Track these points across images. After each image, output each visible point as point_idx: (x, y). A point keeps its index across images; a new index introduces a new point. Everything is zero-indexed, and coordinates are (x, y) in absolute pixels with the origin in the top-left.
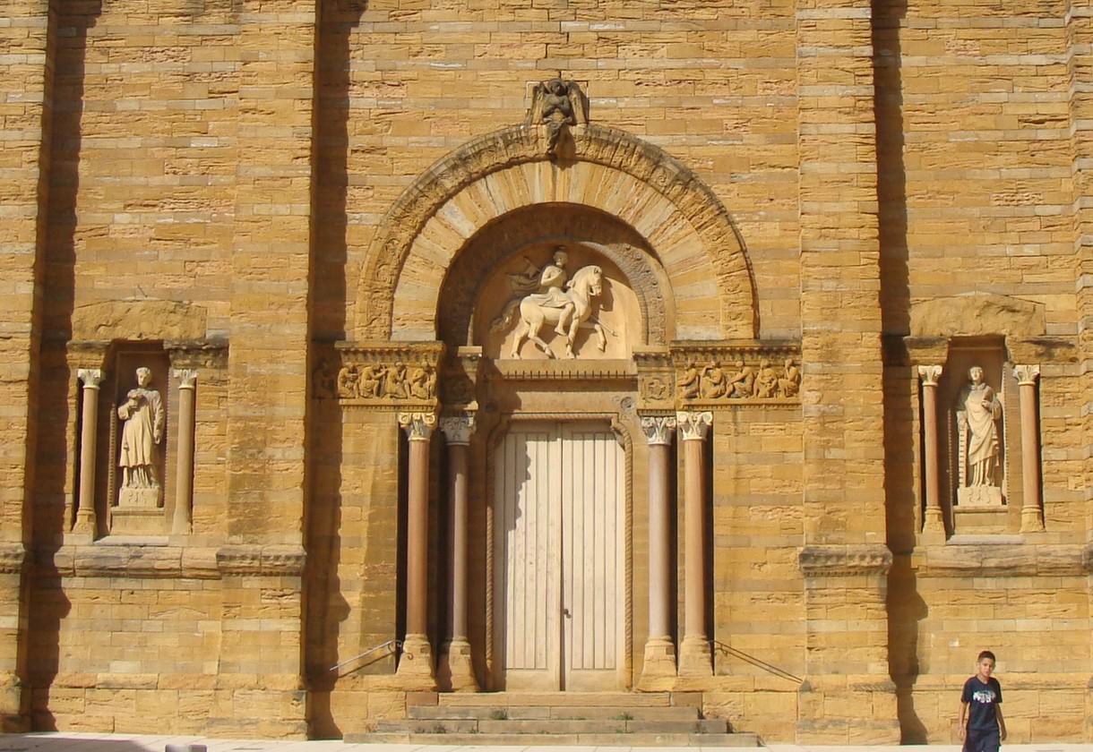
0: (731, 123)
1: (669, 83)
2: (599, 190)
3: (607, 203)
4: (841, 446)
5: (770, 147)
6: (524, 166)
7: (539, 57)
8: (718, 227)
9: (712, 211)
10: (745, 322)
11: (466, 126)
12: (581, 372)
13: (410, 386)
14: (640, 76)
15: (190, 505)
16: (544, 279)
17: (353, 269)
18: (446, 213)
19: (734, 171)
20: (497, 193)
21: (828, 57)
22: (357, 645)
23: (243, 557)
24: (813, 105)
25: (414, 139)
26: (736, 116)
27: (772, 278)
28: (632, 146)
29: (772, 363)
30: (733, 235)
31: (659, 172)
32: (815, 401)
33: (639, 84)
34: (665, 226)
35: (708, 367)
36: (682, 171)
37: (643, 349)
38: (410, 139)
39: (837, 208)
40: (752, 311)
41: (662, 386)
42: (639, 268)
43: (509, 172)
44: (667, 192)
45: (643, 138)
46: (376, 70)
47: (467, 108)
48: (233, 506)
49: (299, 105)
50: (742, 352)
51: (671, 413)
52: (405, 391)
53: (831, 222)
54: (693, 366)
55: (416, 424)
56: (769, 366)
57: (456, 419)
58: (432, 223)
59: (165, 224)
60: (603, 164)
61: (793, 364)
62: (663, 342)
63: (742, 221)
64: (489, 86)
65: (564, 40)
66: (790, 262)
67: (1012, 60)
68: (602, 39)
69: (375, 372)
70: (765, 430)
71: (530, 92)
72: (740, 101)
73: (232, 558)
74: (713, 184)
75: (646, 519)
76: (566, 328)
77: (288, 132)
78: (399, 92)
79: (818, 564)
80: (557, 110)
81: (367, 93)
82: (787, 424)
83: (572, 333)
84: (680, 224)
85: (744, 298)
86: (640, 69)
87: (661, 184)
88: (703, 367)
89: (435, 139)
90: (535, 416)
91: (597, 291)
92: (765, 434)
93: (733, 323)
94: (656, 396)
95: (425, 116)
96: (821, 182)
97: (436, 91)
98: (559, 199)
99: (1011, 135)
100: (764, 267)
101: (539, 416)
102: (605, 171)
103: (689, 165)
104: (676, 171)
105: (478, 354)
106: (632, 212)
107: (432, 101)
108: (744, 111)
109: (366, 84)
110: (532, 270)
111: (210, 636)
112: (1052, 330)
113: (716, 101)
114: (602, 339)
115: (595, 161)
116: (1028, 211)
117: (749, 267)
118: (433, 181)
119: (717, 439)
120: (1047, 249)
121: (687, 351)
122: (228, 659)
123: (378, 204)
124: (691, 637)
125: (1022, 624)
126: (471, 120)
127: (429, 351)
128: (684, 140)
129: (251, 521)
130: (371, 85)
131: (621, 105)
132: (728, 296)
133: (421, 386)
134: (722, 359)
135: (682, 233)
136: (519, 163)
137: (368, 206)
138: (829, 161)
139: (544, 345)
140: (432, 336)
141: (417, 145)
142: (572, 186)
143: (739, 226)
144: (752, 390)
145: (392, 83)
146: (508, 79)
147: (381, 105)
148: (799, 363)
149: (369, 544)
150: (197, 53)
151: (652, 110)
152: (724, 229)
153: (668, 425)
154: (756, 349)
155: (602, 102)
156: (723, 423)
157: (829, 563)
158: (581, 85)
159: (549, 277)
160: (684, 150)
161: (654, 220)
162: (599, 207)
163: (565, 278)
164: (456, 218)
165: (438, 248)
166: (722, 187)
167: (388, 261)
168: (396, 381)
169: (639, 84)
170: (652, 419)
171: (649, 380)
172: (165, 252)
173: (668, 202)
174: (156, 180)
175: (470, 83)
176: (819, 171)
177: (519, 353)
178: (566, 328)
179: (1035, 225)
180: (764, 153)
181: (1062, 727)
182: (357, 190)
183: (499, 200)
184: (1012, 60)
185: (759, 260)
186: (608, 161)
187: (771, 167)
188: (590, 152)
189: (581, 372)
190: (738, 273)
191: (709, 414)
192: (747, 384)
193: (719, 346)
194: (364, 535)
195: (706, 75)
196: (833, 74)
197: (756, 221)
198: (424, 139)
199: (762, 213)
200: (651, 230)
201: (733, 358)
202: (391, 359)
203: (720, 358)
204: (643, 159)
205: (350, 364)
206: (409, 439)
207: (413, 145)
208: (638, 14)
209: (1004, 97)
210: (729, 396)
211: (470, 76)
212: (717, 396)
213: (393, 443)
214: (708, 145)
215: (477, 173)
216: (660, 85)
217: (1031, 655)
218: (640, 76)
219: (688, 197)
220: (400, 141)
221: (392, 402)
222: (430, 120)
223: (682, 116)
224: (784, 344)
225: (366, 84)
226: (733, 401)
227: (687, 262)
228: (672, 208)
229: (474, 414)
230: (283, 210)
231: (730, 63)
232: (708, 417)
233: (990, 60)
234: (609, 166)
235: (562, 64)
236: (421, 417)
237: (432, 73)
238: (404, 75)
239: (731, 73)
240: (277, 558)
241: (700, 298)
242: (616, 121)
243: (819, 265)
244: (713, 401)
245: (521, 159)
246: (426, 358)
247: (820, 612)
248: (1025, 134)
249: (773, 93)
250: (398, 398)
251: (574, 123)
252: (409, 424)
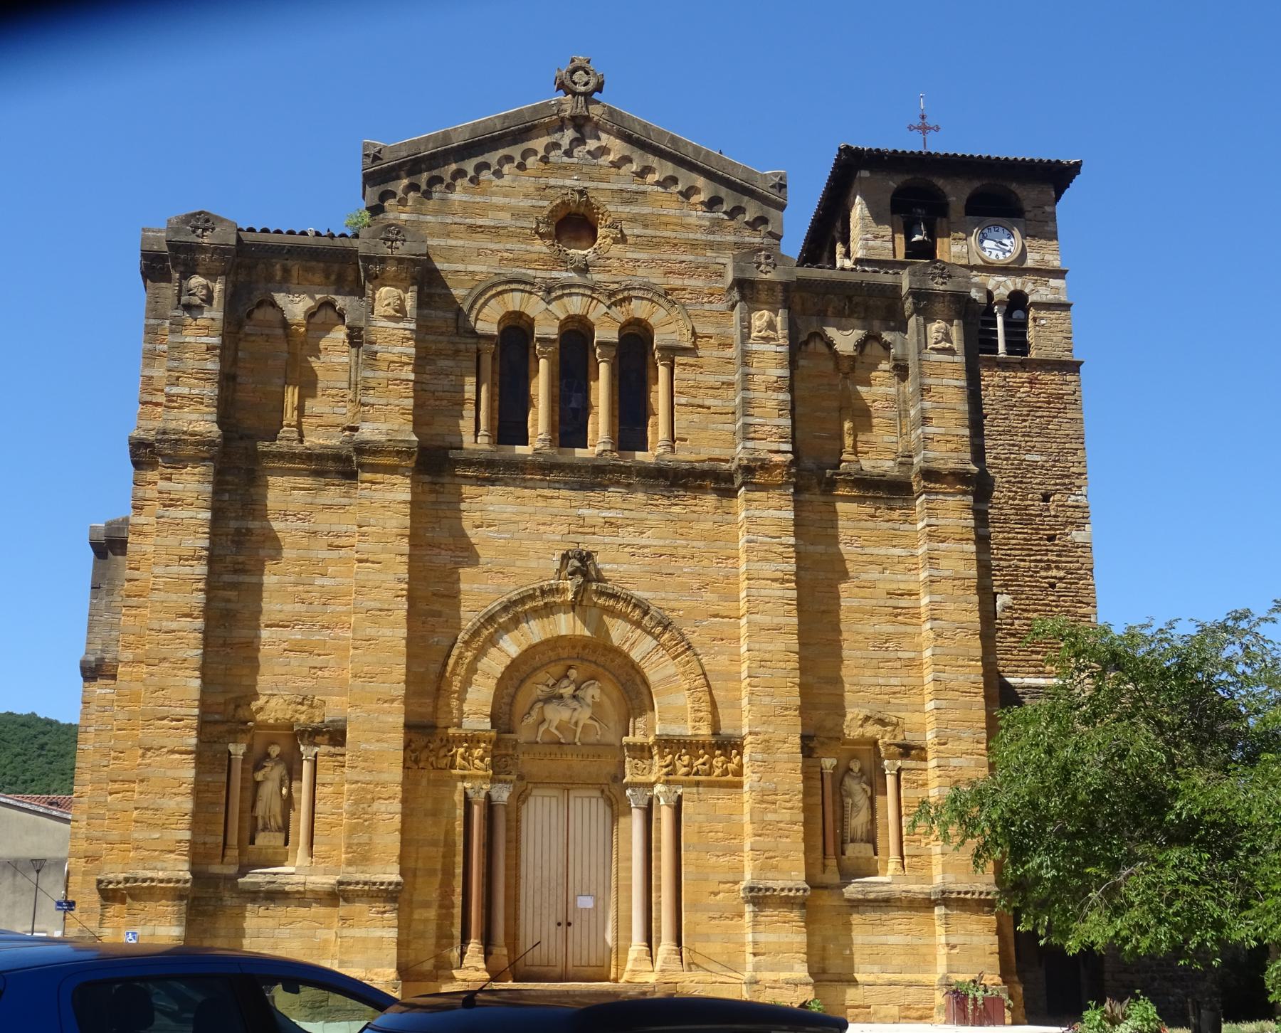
0: (696, 586)
4: (775, 812)
5: (720, 603)
15: (311, 844)
21: (766, 543)
22: (432, 948)
23: (357, 883)
25: (475, 586)
30: (697, 663)
31: (647, 618)
32: (757, 779)
39: (771, 647)
45: (636, 593)
48: (349, 846)
49: (399, 559)
51: (651, 785)
53: (767, 656)
56: (721, 755)
59: (295, 640)
65: (581, 522)
67: (882, 551)
68: (610, 523)
71: (557, 557)
73: (349, 884)
75: (629, 859)
77: (391, 577)
79: (761, 894)
85: (705, 706)
99: (882, 603)
106: (628, 644)
111: (326, 941)
112: (909, 736)
116: (892, 655)
117: (708, 686)
118: (490, 619)
120: (906, 681)
122: (345, 958)
124: (665, 947)
125: (891, 939)
129: (361, 856)
140: (488, 726)
149: (443, 875)
150: (319, 517)
157: (768, 893)
172: (295, 660)
174: (288, 607)
179: (898, 664)
181: (919, 1013)
183: (536, 631)
184: (882, 551)
194: (439, 866)
196: (770, 556)
198: (484, 586)
208: (633, 507)
209: (877, 576)
211: (517, 544)
217: (897, 961)
219: (666, 636)
227: (668, 679)
228: (655, 642)
230: (388, 632)
231: (695, 544)
233: (867, 550)
235: (580, 538)
240: (382, 884)
247: (761, 928)
248: (890, 602)
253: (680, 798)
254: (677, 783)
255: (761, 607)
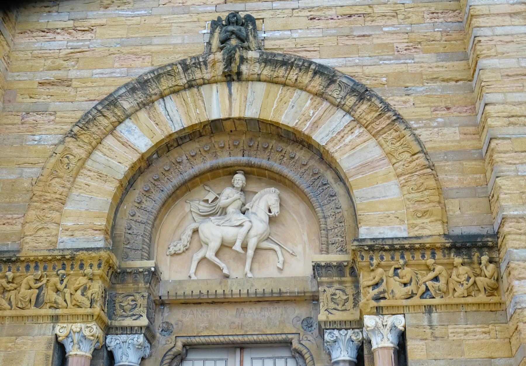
0: (402, 46)
1: (340, 17)
2: (275, 106)
3: (283, 117)
5: (440, 64)
6: (202, 89)
7: (218, 2)
8: (396, 131)
9: (389, 118)
10: (433, 219)
11: (148, 59)
12: (260, 290)
13: (71, 294)
14: (312, 13)
16: (223, 201)
17: (26, 185)
18: (123, 131)
19: (407, 85)
20: (175, 112)
24: (484, 12)
25: (98, 71)
26: (407, 40)
27: (456, 178)
28: (306, 64)
29: (466, 260)
30: (412, 138)
33: (311, 19)
34: (342, 134)
35: (397, 266)
36: (356, 84)
37: (323, 259)
38: (94, 71)
40: (440, 208)
41: (345, 297)
42: (316, 183)
43: (187, 94)
44: (343, 103)
46: (69, 20)
47: (150, 44)
50: (433, 250)
52: (65, 301)
54: (378, 266)
55: (76, 337)
57: (124, 337)
58: (110, 141)
60: (277, 83)
61: (491, 261)
62: (342, 251)
63: (420, 128)
64: (171, 26)
66: (474, 163)
69: (37, 280)
70: (466, 334)
72: (409, 28)
74: (389, 97)
76: (245, 247)
78: (88, 36)
80: (234, 36)
81: (59, 37)
82: (490, 327)
83: (250, 252)
84: (357, 132)
86: (313, 8)
87: (335, 96)
88: (390, 266)
89: (118, 70)
90: (212, 339)
91: (275, 210)
92: (466, 337)
93: (419, 221)
94: (339, 307)
95: (110, 53)
96: (502, 76)
97: (122, 32)
98: (235, 114)
100: (446, 168)
101: (217, 339)
102: (279, 90)
103: (364, 82)
104: (351, 84)
105: (150, 268)
107: (118, 41)
108: (413, 36)
109: (59, 31)
110: (211, 197)
113: (385, 29)
114: (281, 259)
115: (271, 81)
119: (410, 345)
121: (371, 248)
123: (58, 127)
126: (152, 54)
127: (93, 257)
128: (357, 61)
130: (63, 32)
131: (295, 35)
132: (412, 195)
133: (83, 295)
134: (411, 258)
135: (359, 140)
136: (199, 86)
137: (49, 129)
138: (508, 57)
139: (222, 265)
141: (101, 76)
142: (248, 103)
143: (416, 132)
144: (448, 288)
145: (83, 29)
146: (189, 21)
147: (70, 46)
148: (497, 260)
151: (325, 38)
152: (403, 132)
153: (354, 338)
154: (448, 245)
155: (277, 34)
156: (417, 327)
158: (257, 22)
159: (227, 199)
160: (359, 70)
161: (331, 129)
162: (275, 120)
163: (243, 199)
164: (133, 135)
165: (114, 163)
166: (397, 98)
167: (61, 174)
168: (57, 291)
169: (311, 19)
170: (336, 332)
171: (332, 290)
173: (344, 113)
175: (154, 25)
176: (498, 65)
177: (195, 274)
178: (245, 247)
180: (436, 69)
182: (39, 116)
183: (176, 118)
185: (441, 161)
186: (283, 80)
187: (443, 81)
188: (265, 72)
189: (260, 290)
190: (422, 171)
191: (401, 317)
192: (442, 283)
193: (407, 244)
195: (375, 9)
197: (434, 127)
198: (108, 71)
199: (440, 120)
200: (328, 138)
201: (423, 256)
202: (54, 268)
203: (408, 256)
204: (317, 76)
205: (10, 275)
206: (67, 355)
207: (97, 76)
210: (422, 297)
211: (154, 20)
212: (411, 296)
213: (47, 356)
214: (380, 65)
215: (155, 94)
216: (332, 19)
218: (312, 13)
220: (85, 73)
221: (52, 312)
222: (114, 56)
223: (353, 42)
224: (479, 240)
225: (59, 31)
226: (428, 301)
228: (348, 118)
229: (143, 331)
232: (400, 321)
234: (285, 85)
236: (81, 329)
237: (119, 19)
238: (93, 22)
239: (399, 7)
241: (382, 199)
242: (292, 48)
243: (512, 151)
244: (405, 302)
245: (198, 81)
246: (91, 266)
249: (441, 20)
250: (56, 308)
251: (248, 48)
252: (67, 337)
253: (402, 337)
254: (394, 310)
255: (500, 49)
